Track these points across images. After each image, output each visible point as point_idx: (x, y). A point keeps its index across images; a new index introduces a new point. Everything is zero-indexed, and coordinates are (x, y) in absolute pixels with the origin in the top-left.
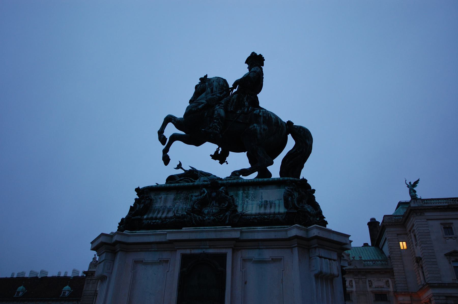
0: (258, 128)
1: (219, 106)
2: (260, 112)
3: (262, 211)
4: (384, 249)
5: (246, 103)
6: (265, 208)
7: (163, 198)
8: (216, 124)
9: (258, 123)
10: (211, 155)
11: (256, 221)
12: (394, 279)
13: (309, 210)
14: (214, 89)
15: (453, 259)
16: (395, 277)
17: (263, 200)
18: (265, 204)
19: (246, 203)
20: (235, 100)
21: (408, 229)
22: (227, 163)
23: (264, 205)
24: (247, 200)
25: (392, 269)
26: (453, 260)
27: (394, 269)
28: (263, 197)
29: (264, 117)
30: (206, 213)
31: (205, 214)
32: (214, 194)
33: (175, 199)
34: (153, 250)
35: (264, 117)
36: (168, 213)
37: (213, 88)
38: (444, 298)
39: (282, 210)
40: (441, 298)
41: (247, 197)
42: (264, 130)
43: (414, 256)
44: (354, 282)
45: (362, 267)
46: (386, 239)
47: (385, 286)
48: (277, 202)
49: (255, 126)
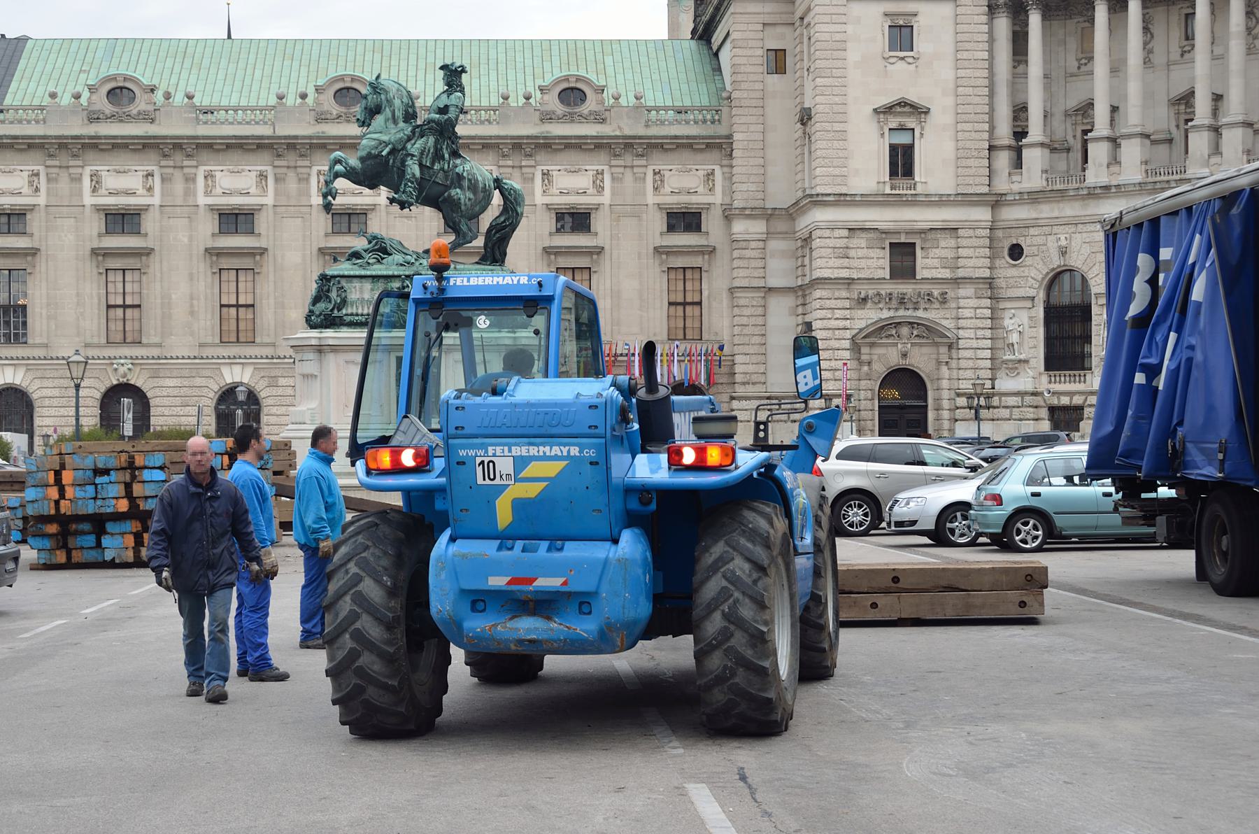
4: (722, 55)
5: (447, 156)
9: (461, 187)
12: (732, 167)
15: (894, 122)
16: (734, 162)
21: (798, 14)
25: (730, 137)
26: (893, 125)
27: (736, 137)
29: (470, 180)
35: (470, 180)
38: (846, 233)
40: (837, 233)
43: (798, 100)
44: (607, 178)
45: (641, 131)
46: (728, 33)
47: (701, 189)
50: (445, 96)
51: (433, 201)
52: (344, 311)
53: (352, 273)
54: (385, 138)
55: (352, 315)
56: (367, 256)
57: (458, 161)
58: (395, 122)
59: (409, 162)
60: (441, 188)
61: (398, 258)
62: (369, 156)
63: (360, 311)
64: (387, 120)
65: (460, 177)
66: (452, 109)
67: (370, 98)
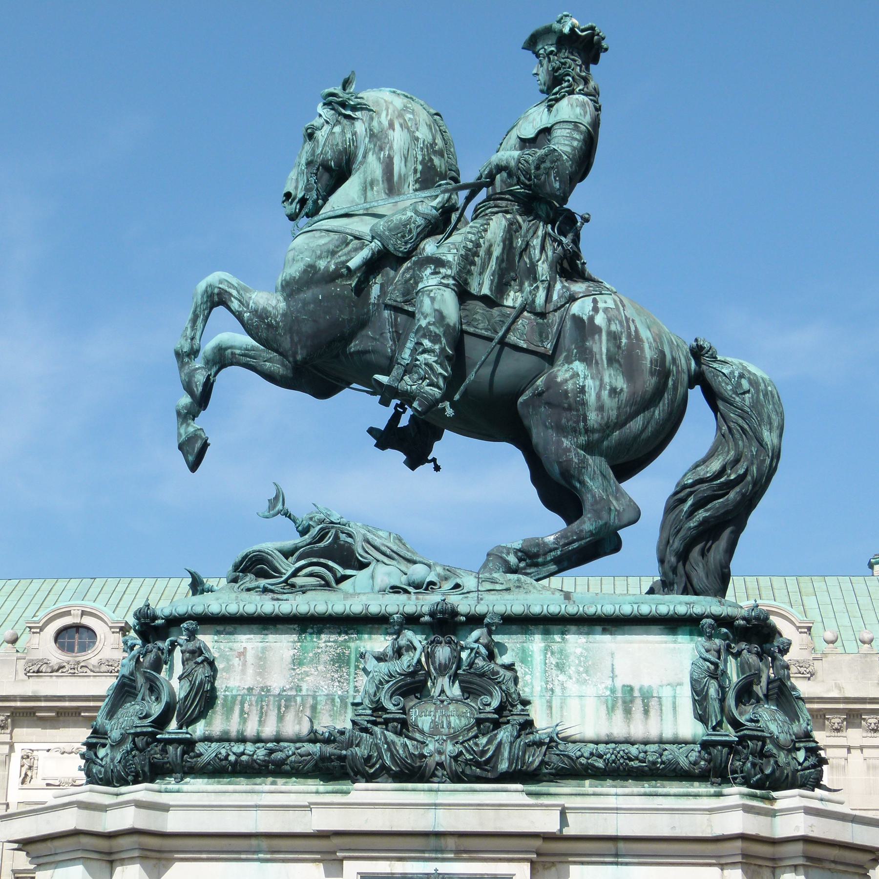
1: (435, 273)
2: (596, 309)
3: (618, 728)
5: (543, 269)
6: (628, 712)
7: (250, 657)
8: (431, 358)
10: (372, 431)
11: (600, 764)
13: (773, 728)
14: (398, 166)
17: (619, 684)
18: (627, 700)
19: (558, 691)
20: (497, 251)
22: (437, 468)
23: (624, 702)
24: (562, 677)
28: (617, 672)
29: (614, 337)
30: (426, 729)
31: (422, 732)
32: (443, 653)
33: (297, 662)
34: (261, 856)
35: (614, 337)
36: (281, 718)
37: (390, 159)
39: (689, 727)
41: (560, 667)
42: (614, 392)
48: (666, 693)
49: (576, 375)
50: (543, 108)
51: (496, 415)
52: (199, 729)
53: (233, 609)
54: (362, 226)
55: (224, 739)
56: (287, 567)
57: (578, 287)
58: (392, 187)
59: (429, 280)
60: (526, 362)
61: (386, 573)
62: (311, 277)
63: (251, 730)
64: (368, 186)
65: (584, 328)
66: (559, 133)
67: (321, 135)
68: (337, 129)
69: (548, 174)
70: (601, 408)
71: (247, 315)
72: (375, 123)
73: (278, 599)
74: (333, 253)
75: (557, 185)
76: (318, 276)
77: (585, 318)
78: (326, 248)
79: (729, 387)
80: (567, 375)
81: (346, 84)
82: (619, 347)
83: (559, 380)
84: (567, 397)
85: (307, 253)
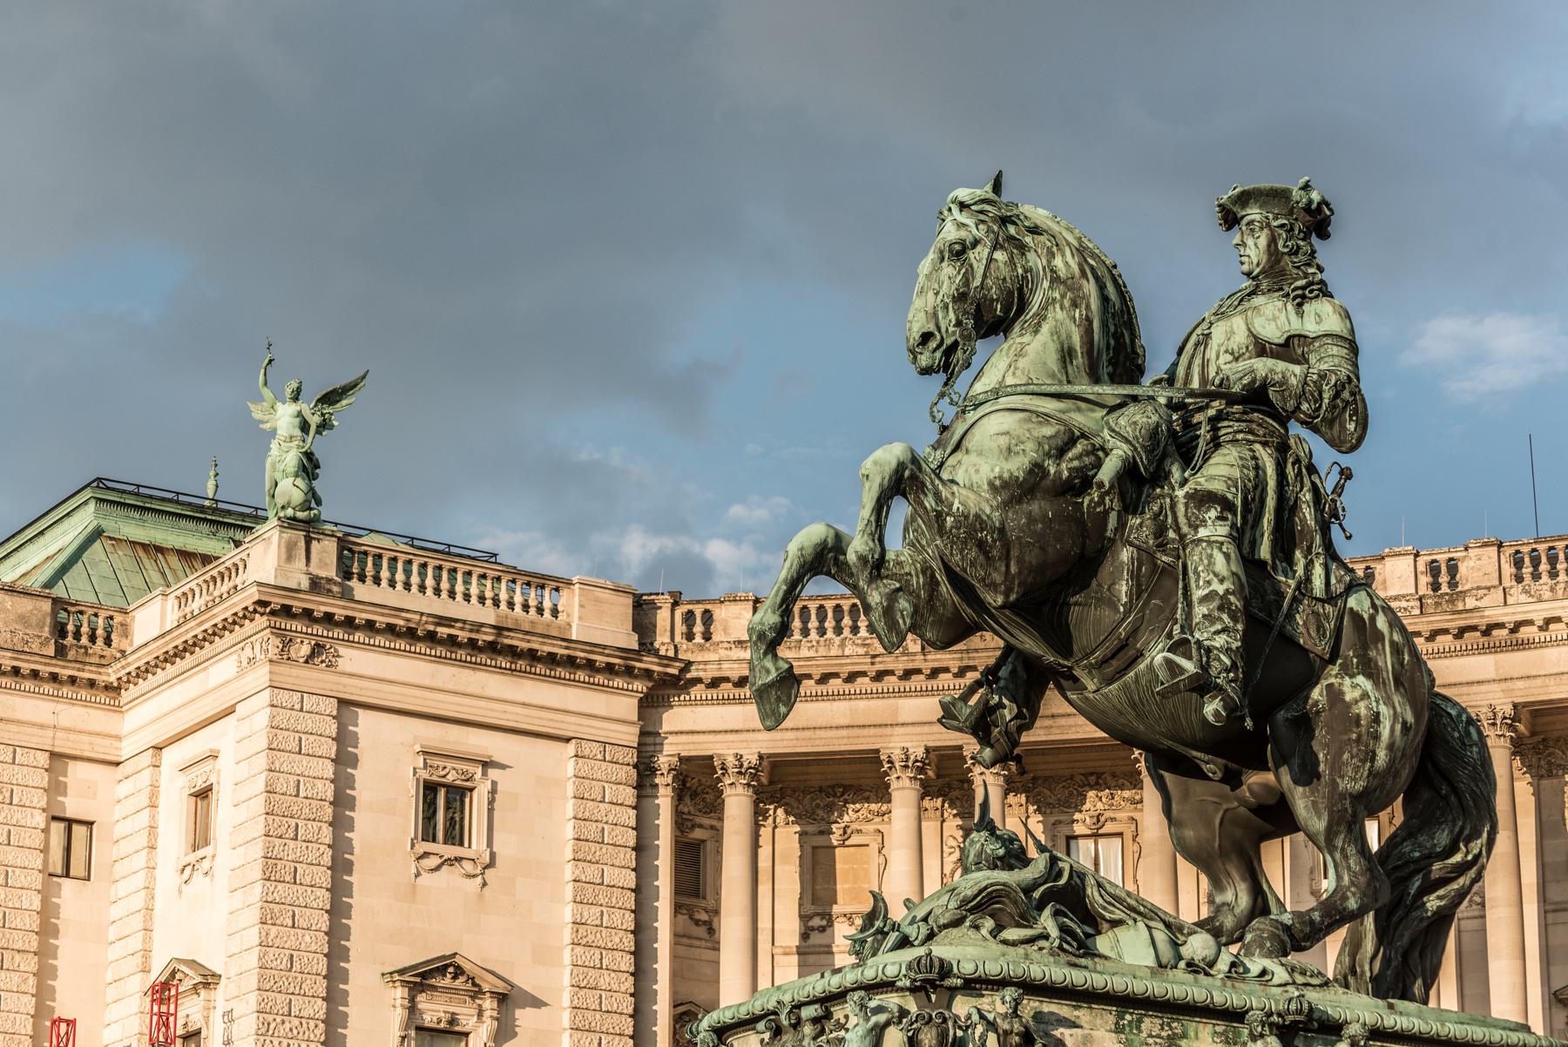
0: (1383, 709)
1: (1221, 518)
2: (1374, 606)
20: (1271, 502)
37: (1089, 320)
42: (1404, 723)
49: (1365, 696)
64: (1066, 355)
65: (1366, 633)
68: (1000, 256)
69: (1344, 408)
70: (1391, 747)
71: (949, 520)
72: (1058, 262)
73: (1075, 965)
74: (1061, 452)
75: (1351, 427)
76: (1047, 482)
77: (1366, 616)
78: (1054, 443)
79: (1456, 735)
80: (1357, 694)
81: (997, 187)
82: (1402, 664)
83: (1348, 698)
84: (1358, 724)
85: (1030, 446)
